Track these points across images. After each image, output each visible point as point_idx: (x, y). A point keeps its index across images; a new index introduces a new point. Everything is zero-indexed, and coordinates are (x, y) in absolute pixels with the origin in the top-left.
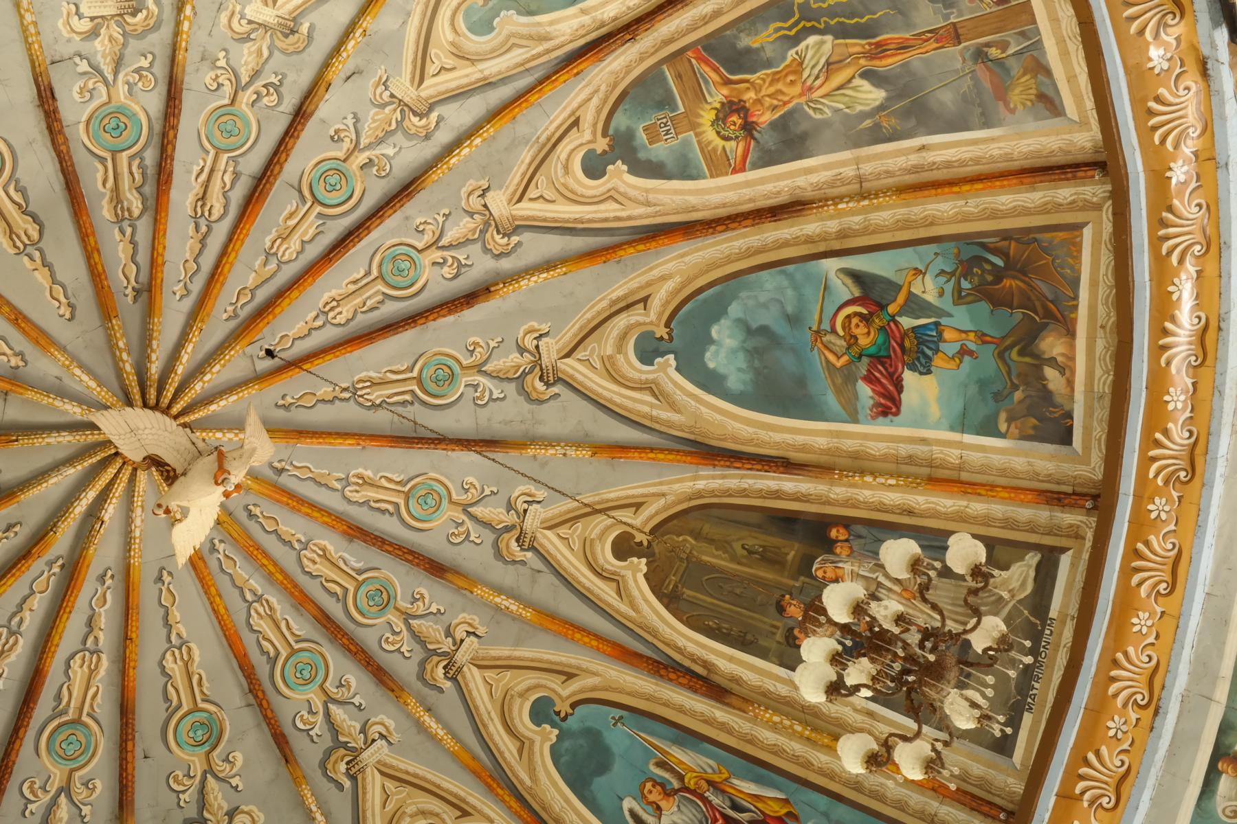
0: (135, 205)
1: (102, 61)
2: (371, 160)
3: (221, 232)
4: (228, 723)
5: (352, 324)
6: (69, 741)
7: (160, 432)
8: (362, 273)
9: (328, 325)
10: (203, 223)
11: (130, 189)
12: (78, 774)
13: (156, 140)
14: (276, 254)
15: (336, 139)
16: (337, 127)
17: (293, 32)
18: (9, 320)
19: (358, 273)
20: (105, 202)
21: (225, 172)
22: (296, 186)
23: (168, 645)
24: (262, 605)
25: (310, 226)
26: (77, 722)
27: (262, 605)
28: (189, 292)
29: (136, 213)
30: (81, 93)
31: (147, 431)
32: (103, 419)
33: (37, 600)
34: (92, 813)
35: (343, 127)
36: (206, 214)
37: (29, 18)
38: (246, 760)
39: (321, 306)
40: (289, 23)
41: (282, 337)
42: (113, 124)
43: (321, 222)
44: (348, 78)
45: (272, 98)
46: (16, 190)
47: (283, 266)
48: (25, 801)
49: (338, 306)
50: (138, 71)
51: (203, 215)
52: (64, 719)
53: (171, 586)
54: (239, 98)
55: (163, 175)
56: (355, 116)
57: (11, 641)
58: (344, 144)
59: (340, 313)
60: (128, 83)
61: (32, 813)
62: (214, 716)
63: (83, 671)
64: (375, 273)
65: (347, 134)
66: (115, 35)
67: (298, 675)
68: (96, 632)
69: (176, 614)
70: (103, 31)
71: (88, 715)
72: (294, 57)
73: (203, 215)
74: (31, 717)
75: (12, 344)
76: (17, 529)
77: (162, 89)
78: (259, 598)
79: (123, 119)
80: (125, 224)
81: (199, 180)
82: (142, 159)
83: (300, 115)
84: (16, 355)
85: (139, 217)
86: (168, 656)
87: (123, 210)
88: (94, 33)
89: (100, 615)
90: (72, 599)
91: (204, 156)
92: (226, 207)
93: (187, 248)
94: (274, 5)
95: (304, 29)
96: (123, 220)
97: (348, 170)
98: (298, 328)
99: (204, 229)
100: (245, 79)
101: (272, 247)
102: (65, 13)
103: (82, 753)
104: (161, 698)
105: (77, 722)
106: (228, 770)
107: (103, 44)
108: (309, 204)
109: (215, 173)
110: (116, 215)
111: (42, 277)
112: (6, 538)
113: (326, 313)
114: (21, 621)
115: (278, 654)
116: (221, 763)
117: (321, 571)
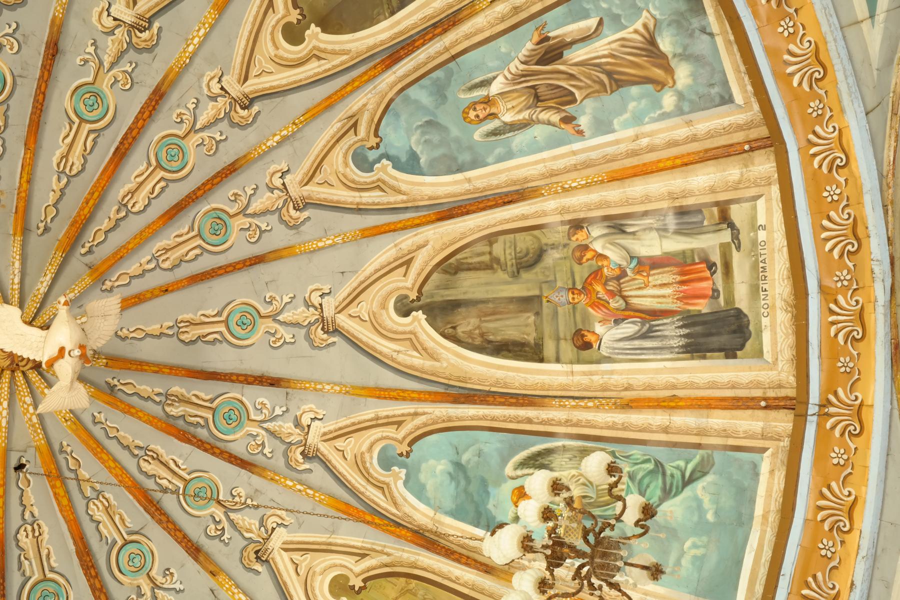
0: (173, 410)
1: (278, 424)
2: (143, 595)
3: (130, 464)
5: (14, 543)
8: (54, 564)
9: (22, 523)
10: (141, 453)
11: (185, 411)
13: (212, 441)
14: (97, 499)
15: (167, 572)
16: (176, 575)
17: (258, 558)
18: (140, 294)
19: (55, 561)
20: (183, 391)
21: (170, 482)
22: (142, 531)
25: (109, 532)
28: (95, 423)
29: (168, 409)
30: (262, 403)
35: (174, 580)
36: (146, 458)
37: (328, 387)
39: (40, 522)
40: (266, 557)
41: (29, 481)
42: (233, 416)
43: (109, 542)
44: (212, 591)
45: (213, 532)
46: (215, 339)
47: (86, 501)
49: (34, 536)
50: (263, 444)
51: (146, 455)
54: (220, 507)
55: (185, 437)
56: (181, 591)
58: (161, 578)
59: (27, 536)
60: (257, 435)
64: (50, 575)
65: (169, 581)
66: (292, 438)
70: (298, 431)
72: (238, 555)
73: (146, 455)
75: (121, 288)
77: (246, 457)
79: (234, 424)
80: (163, 399)
81: (171, 461)
82: (203, 427)
83: (195, 551)
84: (112, 287)
85: (163, 409)
87: (173, 400)
88: (297, 424)
91: (188, 471)
92: (146, 474)
93: (127, 435)
94: (282, 549)
95: (258, 567)
96: (167, 398)
97: (142, 574)
98: (31, 497)
99: (136, 452)
100: (232, 516)
101: (104, 497)
102: (318, 411)
107: (288, 428)
108: (126, 536)
109: (171, 474)
110: (173, 395)
111: (154, 328)
113: (32, 525)
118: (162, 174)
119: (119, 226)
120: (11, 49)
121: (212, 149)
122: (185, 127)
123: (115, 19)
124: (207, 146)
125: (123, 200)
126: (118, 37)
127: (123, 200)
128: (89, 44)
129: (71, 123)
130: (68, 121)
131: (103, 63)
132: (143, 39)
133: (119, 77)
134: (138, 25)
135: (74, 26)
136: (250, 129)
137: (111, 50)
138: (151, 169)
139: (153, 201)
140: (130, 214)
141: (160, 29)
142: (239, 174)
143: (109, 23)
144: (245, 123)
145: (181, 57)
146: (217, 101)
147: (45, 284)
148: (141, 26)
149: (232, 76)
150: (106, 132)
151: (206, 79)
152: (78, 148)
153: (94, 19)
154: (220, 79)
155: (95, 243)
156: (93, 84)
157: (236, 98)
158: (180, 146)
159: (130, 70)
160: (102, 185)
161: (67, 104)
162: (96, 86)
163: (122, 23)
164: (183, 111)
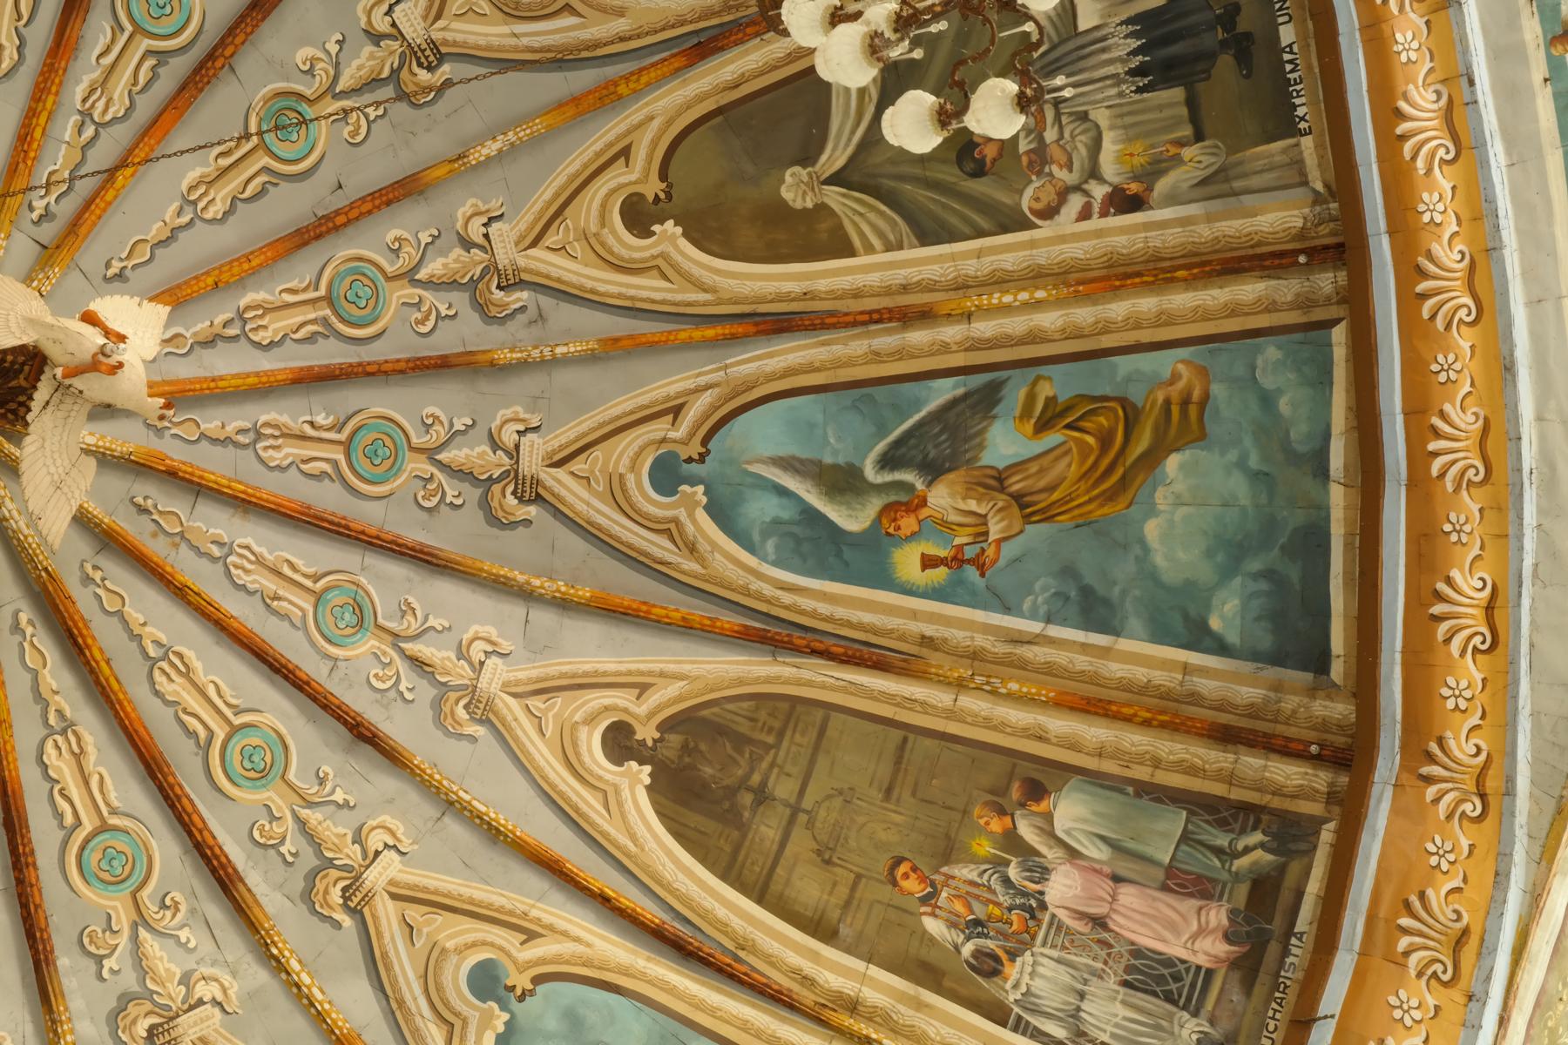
4: (265, 90)
6: (355, 299)
7: (48, 453)
12: (389, 269)
23: (197, 221)
24: (93, 106)
26: (329, 299)
27: (93, 106)
31: (52, 470)
32: (54, 529)
33: (208, 426)
34: (427, 228)
38: (305, 42)
48: (440, 322)
52: (333, 320)
53: (124, 256)
57: (268, 431)
61: (449, 308)
62: (262, 114)
63: (271, 322)
67: (168, 10)
68: (218, 329)
69: (155, 231)
71: (316, 289)
74: (351, 365)
76: (139, 500)
78: (86, 114)
86: (209, 215)
89: (195, 334)
90: (198, 386)
103: (364, 275)
104: (266, 199)
105: (329, 299)
106: (321, 65)
112: (155, 506)
114: (240, 431)
115: (149, 53)
116: (318, 78)
117: (9, 29)
118: (88, 826)
119: (36, 702)
120: (376, 676)
121: (91, 942)
122: (151, 908)
123: (377, 853)
124: (100, 935)
125: (75, 733)
126: (347, 847)
127: (75, 733)
128: (347, 797)
129: (238, 711)
130: (243, 706)
131: (309, 808)
132: (331, 889)
133: (278, 827)
134: (357, 889)
135: (387, 783)
136: (105, 1030)
137: (328, 829)
138: (105, 812)
139: (48, 786)
140: (45, 732)
141: (337, 925)
142: (23, 978)
143: (375, 841)
144: (121, 1025)
145: (285, 942)
146: (180, 983)
147: (15, 513)
148: (354, 894)
149: (216, 1030)
150: (199, 761)
151: (226, 979)
152: (192, 702)
153: (387, 819)
154: (219, 1004)
155: (26, 644)
156: (283, 777)
157: (176, 1022)
158: (123, 881)
159: (283, 849)
160: (126, 704)
161: (267, 719)
162: (278, 780)
163: (367, 862)
164: (179, 916)
